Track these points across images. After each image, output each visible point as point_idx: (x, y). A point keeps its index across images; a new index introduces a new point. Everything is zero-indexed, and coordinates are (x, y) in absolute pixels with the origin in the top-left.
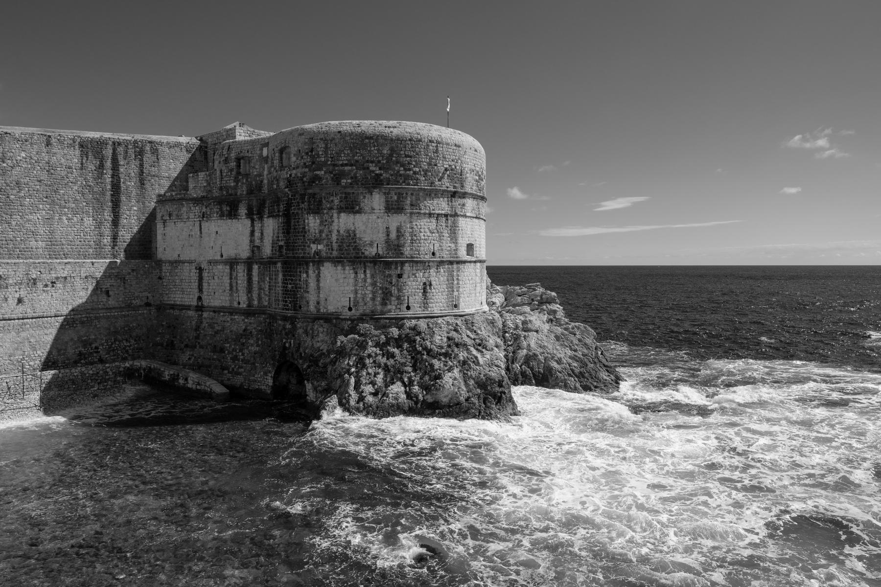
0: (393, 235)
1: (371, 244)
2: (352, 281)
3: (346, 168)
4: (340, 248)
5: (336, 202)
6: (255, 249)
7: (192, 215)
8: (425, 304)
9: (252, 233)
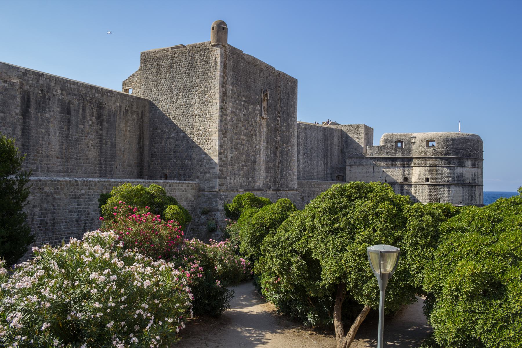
0: (473, 175)
1: (468, 179)
2: (462, 192)
3: (461, 150)
4: (458, 180)
5: (456, 162)
6: (406, 179)
7: (369, 164)
8: (480, 202)
9: (404, 172)
